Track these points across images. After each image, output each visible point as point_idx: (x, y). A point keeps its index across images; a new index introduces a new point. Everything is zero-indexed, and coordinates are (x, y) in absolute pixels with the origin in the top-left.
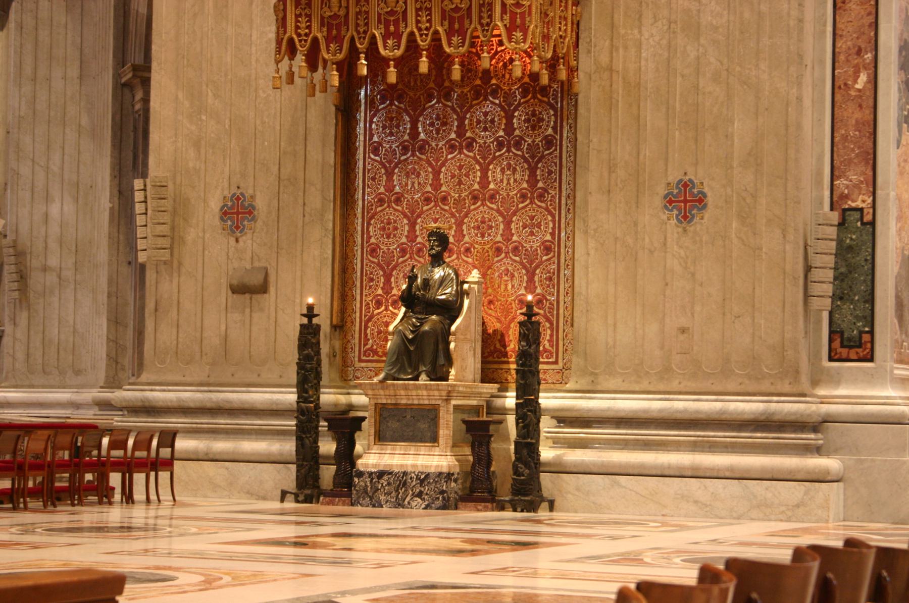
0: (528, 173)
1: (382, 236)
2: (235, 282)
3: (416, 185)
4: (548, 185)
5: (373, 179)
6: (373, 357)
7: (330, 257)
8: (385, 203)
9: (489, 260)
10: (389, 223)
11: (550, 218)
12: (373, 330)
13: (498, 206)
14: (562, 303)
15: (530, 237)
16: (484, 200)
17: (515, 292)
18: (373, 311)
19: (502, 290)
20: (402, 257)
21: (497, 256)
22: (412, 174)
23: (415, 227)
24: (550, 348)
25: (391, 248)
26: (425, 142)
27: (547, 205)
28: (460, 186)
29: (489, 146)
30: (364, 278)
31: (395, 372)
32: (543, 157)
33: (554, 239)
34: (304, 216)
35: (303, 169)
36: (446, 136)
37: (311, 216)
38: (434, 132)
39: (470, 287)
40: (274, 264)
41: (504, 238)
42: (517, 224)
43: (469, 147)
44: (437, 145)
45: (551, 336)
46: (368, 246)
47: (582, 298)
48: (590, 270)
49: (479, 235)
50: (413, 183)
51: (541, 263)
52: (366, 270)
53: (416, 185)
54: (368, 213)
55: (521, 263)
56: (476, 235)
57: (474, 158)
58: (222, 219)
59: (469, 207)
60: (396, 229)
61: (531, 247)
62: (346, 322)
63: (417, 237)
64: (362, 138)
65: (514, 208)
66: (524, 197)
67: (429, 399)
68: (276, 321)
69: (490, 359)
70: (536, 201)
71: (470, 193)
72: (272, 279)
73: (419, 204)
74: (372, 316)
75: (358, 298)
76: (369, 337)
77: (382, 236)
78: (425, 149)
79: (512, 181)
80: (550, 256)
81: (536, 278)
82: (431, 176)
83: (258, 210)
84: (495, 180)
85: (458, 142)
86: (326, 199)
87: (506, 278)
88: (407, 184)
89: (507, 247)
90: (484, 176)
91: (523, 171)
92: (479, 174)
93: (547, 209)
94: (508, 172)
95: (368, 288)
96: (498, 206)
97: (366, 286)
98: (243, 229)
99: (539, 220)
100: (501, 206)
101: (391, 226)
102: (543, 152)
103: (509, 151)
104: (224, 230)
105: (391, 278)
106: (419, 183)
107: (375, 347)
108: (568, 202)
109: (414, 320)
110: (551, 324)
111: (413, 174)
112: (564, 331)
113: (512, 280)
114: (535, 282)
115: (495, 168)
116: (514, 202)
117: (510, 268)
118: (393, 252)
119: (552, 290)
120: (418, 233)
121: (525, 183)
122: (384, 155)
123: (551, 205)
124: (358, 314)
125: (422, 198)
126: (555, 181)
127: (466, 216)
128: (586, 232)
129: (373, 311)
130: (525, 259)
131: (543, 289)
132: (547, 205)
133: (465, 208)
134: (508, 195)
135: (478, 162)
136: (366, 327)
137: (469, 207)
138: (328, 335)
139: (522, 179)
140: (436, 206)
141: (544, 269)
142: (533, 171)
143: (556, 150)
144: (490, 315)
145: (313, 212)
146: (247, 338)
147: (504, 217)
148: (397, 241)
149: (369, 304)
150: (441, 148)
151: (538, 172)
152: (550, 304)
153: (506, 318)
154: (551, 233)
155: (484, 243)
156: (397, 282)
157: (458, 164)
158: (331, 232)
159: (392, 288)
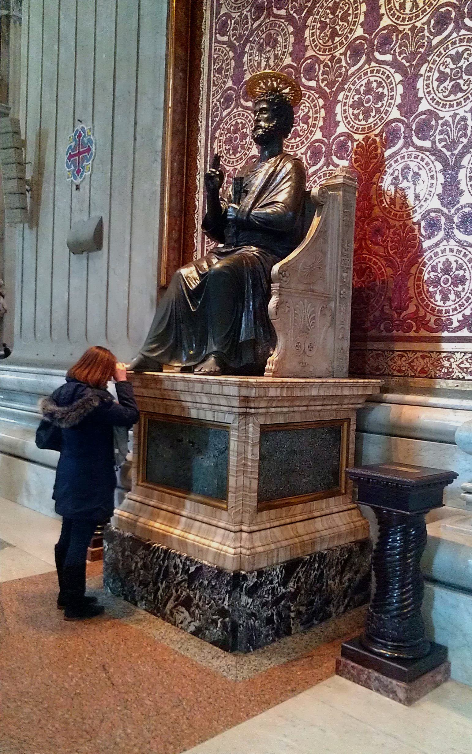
5: (219, 71)
10: (235, 132)
13: (394, 55)
15: (452, 97)
19: (397, 208)
22: (268, 44)
54: (213, 121)
88: (259, 64)
106: (276, 56)
116: (423, 37)
144: (376, 254)
147: (404, 73)
153: (402, 258)
155: (370, 128)
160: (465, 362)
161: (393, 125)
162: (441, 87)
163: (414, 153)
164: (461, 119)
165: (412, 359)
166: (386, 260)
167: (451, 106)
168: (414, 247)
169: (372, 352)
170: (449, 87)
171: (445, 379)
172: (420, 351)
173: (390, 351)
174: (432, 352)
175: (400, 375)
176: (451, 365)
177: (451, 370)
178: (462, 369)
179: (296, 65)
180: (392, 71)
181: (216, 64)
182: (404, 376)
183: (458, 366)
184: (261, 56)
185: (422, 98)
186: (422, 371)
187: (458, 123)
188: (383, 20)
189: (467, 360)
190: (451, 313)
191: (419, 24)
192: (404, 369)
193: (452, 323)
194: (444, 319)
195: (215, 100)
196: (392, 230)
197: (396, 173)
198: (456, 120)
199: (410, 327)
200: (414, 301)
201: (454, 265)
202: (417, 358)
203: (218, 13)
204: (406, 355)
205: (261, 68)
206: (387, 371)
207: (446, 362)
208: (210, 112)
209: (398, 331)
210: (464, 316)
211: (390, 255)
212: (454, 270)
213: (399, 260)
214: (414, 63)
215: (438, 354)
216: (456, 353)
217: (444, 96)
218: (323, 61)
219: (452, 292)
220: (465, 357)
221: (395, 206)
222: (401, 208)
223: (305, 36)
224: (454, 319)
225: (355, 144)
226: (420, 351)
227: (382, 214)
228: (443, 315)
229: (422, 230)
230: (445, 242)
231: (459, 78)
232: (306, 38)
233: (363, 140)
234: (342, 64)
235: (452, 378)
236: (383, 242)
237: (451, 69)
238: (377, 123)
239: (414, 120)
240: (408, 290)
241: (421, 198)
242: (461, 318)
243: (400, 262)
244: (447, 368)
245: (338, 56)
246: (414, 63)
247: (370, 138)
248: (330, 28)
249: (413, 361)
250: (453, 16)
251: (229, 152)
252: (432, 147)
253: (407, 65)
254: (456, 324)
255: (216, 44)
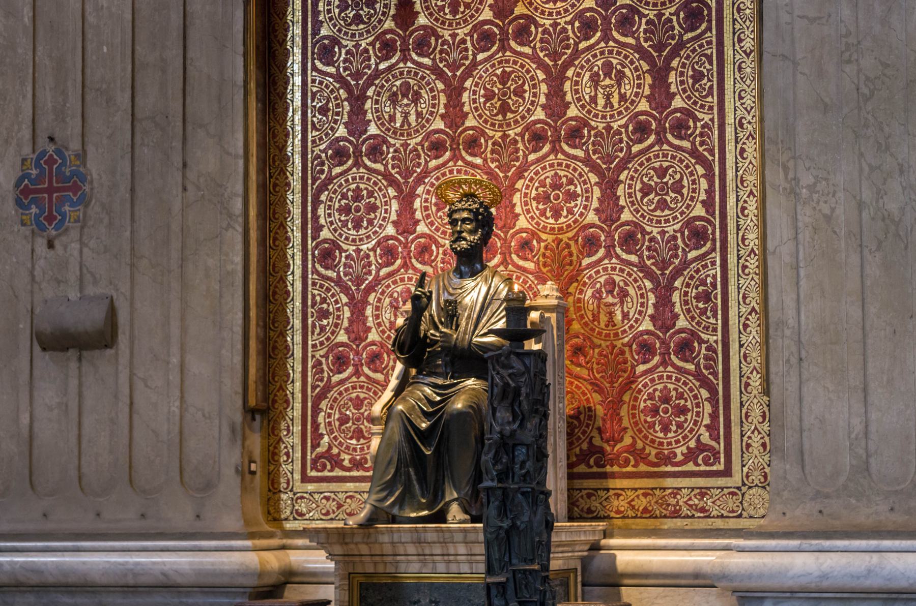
0: (649, 80)
1: (345, 224)
2: (46, 327)
3: (412, 118)
4: (695, 103)
5: (324, 111)
6: (331, 470)
7: (240, 268)
8: (349, 157)
9: (571, 264)
11: (700, 170)
12: (329, 416)
13: (587, 151)
14: (734, 347)
15: (658, 213)
16: (557, 140)
17: (631, 327)
18: (329, 378)
19: (602, 325)
20: (388, 264)
21: (589, 255)
23: (412, 203)
24: (713, 443)
25: (364, 247)
26: (430, 31)
27: (693, 143)
28: (504, 116)
29: (564, 30)
30: (310, 310)
31: (393, 504)
32: (681, 45)
33: (713, 215)
34: (185, 189)
35: (181, 95)
36: (472, 16)
37: (198, 188)
38: (447, 10)
39: (542, 317)
40: (125, 288)
41: (603, 216)
42: (630, 187)
43: (522, 35)
44: (454, 36)
45: (714, 416)
46: (316, 247)
47: (788, 332)
48: (802, 273)
49: (548, 214)
50: (406, 115)
51: (686, 264)
52: (314, 296)
53: (412, 118)
54: (314, 180)
55: (642, 267)
56: (543, 213)
57: (534, 58)
58: (19, 203)
59: (526, 156)
60: (373, 208)
61: (663, 233)
62: (274, 401)
63: (417, 222)
64: (298, 30)
65: (621, 155)
66: (642, 130)
67: (470, 562)
68: (131, 404)
69: (582, 468)
70: (670, 137)
71: (527, 129)
72: (123, 317)
73: (419, 157)
74: (328, 388)
75: (298, 352)
76: (322, 430)
77: (345, 224)
78: (429, 45)
79: (615, 100)
80: (704, 250)
81: (676, 297)
82: (443, 99)
83: (91, 182)
84: (579, 100)
85: (497, 26)
86: (229, 154)
87: (610, 299)
88: (392, 118)
89: (406, 246)
90: (556, 92)
91: (639, 78)
92: (544, 88)
93: (694, 153)
94: (608, 82)
95: (317, 330)
96: (587, 151)
97: (314, 326)
98: (62, 221)
99: (678, 177)
100: (595, 152)
101: (362, 204)
102: (681, 36)
103: (606, 37)
104: (23, 224)
105: (364, 309)
106: (419, 115)
107: (335, 451)
108: (741, 135)
109: (428, 390)
110: (713, 391)
111: (405, 95)
112: (742, 405)
113: (622, 303)
114: (673, 305)
115: (579, 75)
116: (621, 141)
117: (617, 279)
118: (368, 256)
119: (712, 320)
120: (418, 215)
121: (644, 100)
122: (345, 61)
123: (702, 143)
124: (298, 385)
125: (426, 144)
126: (710, 92)
127: (520, 175)
128: (793, 193)
129: (329, 378)
130: (649, 258)
131: (693, 318)
132: (693, 143)
133: (517, 159)
134: (608, 128)
135: (542, 65)
136: (316, 410)
137: (526, 156)
138: (239, 428)
139: (637, 95)
140: (455, 158)
141: (692, 278)
142: (660, 75)
143: (709, 29)
145: (202, 180)
146: (73, 440)
148: (376, 232)
149: (320, 363)
150: (463, 41)
151: (672, 78)
152: (707, 349)
153: (612, 383)
154: (703, 203)
155: (561, 229)
156: (377, 317)
157: (499, 72)
158: (241, 220)
159: (369, 330)
160: (693, 498)
161: (591, 230)
162: (645, 200)
163: (619, 266)
164: (670, 238)
165: (632, 498)
166: (591, 384)
167: (659, 222)
168: (625, 372)
169: (722, 490)
170: (655, 201)
171: (672, 518)
172: (641, 489)
173: (604, 489)
174: (656, 489)
175: (618, 516)
176: (678, 502)
177: (678, 508)
178: (691, 506)
179: (451, 132)
180: (586, 170)
181: (316, 100)
182: (623, 517)
183: (686, 503)
184: (395, 108)
185: (623, 207)
186: (645, 510)
187: (668, 242)
188: (570, 109)
189: (695, 496)
190: (674, 446)
191: (615, 126)
192: (622, 509)
193: (675, 455)
194: (666, 452)
195: (317, 150)
196: (597, 351)
197: (598, 285)
198: (666, 238)
199: (627, 462)
200: (630, 432)
201: (673, 393)
202: (638, 496)
203: (316, 32)
204: (624, 493)
205: (395, 123)
206: (602, 513)
207: (672, 499)
208: (310, 165)
209: (612, 466)
210: (688, 448)
211: (596, 379)
212: (674, 399)
213: (608, 385)
214: (613, 166)
215: (662, 491)
216: (683, 490)
217: (649, 210)
218: (492, 137)
219: (674, 423)
220: (693, 493)
221: (599, 322)
222: (607, 326)
223: (463, 101)
224: (678, 451)
225: (543, 244)
226: (641, 489)
227: (582, 331)
228: (665, 447)
229: (634, 354)
230: (661, 369)
231: (665, 194)
232: (464, 103)
233: (553, 241)
234: (519, 146)
235: (679, 517)
236: (587, 363)
237: (656, 183)
238: (569, 226)
239: (616, 229)
240: (620, 420)
241: (631, 317)
242: (685, 451)
243: (610, 387)
244: (674, 506)
245: (513, 135)
246: (613, 166)
247: (561, 240)
248: (499, 99)
249: (633, 500)
250: (654, 127)
251: (347, 225)
252: (640, 263)
253: (604, 166)
254: (680, 458)
255: (314, 74)
